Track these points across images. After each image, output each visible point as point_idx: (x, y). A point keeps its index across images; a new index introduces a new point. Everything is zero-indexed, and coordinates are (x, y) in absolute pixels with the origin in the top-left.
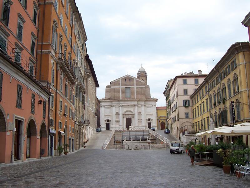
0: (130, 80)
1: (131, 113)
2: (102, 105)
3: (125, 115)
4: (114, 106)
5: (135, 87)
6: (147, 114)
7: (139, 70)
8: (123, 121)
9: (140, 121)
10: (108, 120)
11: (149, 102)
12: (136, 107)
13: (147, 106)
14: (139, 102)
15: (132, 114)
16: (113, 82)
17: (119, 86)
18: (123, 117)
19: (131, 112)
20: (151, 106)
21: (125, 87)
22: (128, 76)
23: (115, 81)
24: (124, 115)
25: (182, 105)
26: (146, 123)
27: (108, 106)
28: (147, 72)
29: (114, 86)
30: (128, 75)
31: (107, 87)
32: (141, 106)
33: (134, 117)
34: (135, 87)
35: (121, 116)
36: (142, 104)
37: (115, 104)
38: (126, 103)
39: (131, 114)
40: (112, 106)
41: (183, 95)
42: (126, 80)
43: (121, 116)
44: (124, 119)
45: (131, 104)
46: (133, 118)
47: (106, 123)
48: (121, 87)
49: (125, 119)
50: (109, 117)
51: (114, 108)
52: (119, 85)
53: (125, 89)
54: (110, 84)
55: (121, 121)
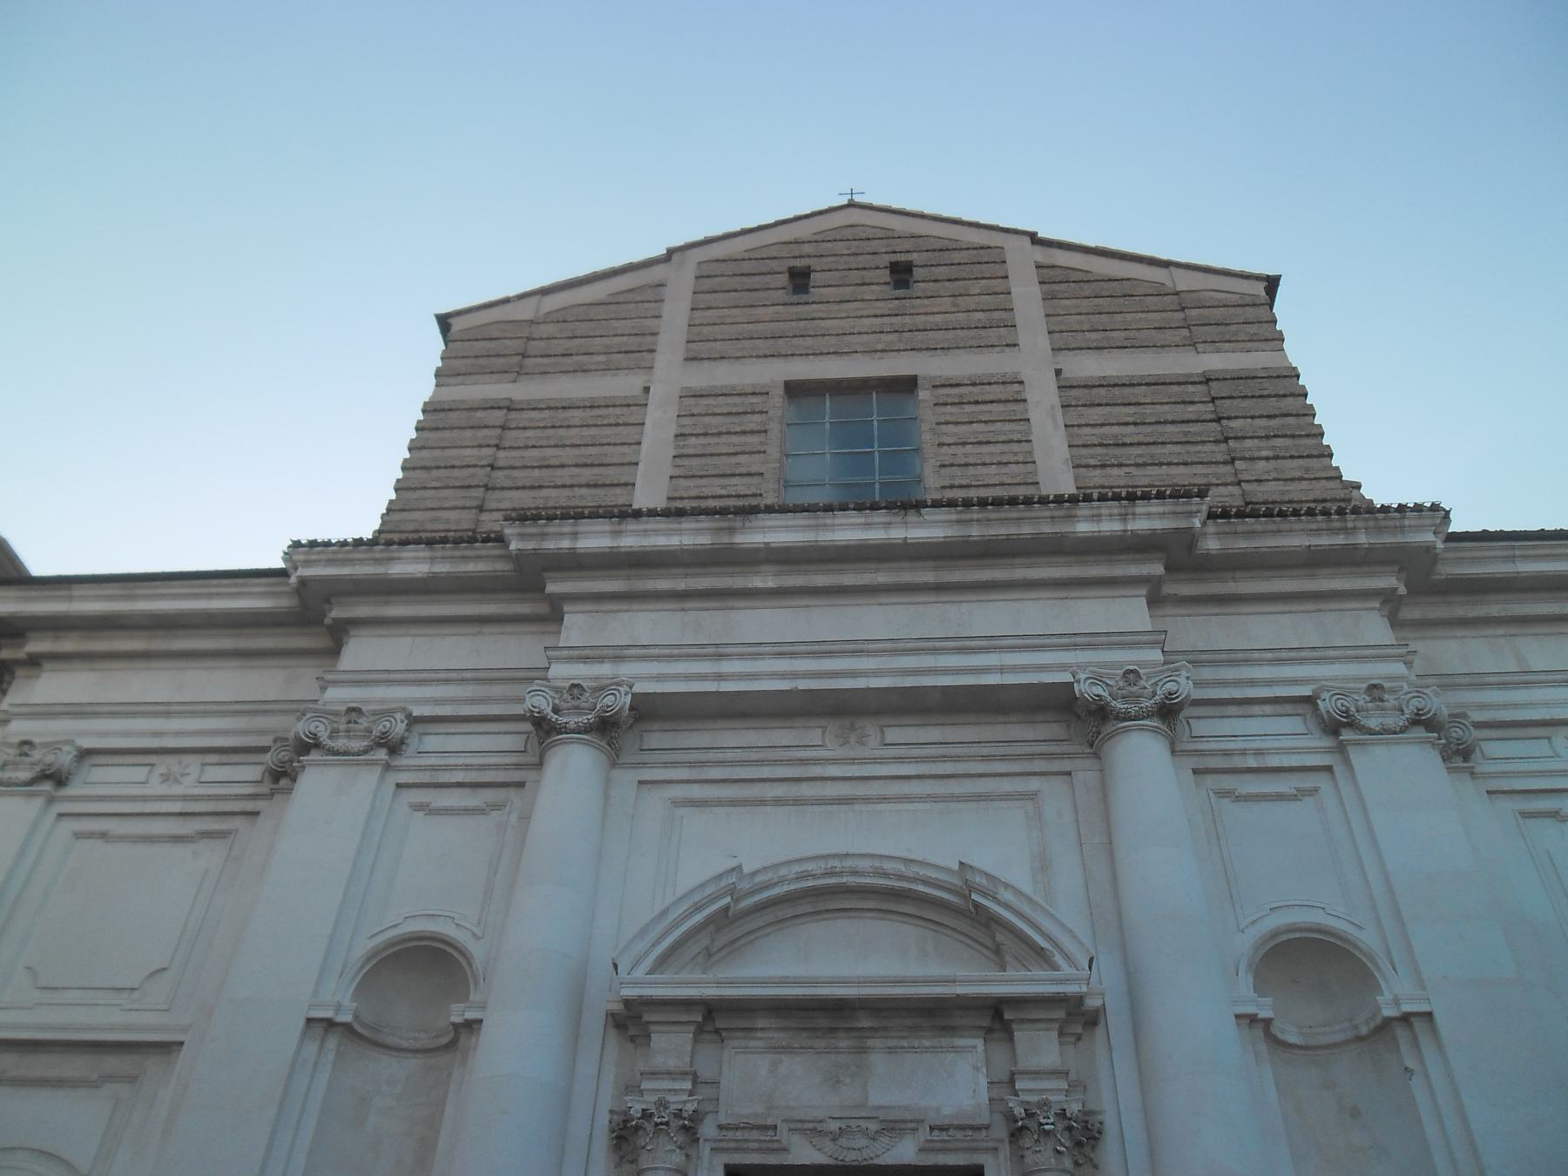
3: (716, 1018)
15: (997, 1017)
22: (855, 217)
24: (671, 1046)
27: (193, 778)
29: (519, 373)
30: (852, 205)
34: (1033, 361)
38: (768, 643)
39: (933, 1016)
42: (800, 279)
48: (670, 375)
52: (640, 353)
53: (778, 393)
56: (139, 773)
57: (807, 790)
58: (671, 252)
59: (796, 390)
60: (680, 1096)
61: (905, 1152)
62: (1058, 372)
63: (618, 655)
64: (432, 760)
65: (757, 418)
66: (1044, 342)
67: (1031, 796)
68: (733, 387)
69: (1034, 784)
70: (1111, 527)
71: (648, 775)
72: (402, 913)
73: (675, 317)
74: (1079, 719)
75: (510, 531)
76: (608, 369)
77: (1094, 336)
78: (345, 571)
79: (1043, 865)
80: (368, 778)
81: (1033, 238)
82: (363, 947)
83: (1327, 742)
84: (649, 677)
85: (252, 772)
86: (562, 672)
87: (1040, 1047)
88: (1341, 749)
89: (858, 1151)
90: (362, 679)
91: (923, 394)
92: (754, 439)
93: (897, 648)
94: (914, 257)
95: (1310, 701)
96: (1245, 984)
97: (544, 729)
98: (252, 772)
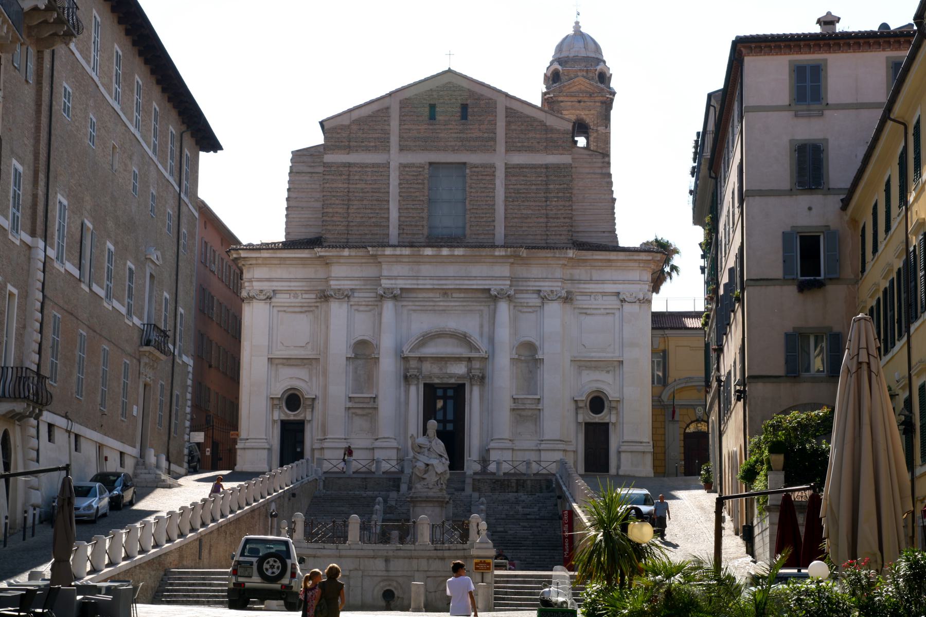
0: (464, 107)
1: (463, 352)
2: (266, 286)
3: (421, 359)
4: (346, 296)
5: (500, 159)
6: (583, 364)
7: (560, 48)
8: (402, 406)
9: (527, 412)
10: (293, 400)
11: (596, 275)
12: (503, 307)
13: (581, 301)
14: (522, 271)
15: (469, 359)
16: (338, 122)
17: (387, 149)
18: (407, 379)
19: (463, 339)
20: (613, 302)
21: (421, 158)
23: (355, 115)
25: (778, 273)
26: (572, 426)
28: (612, 60)
29: (349, 149)
30: (450, 71)
31: (300, 157)
32: (534, 300)
33: (482, 379)
34: (500, 159)
35: (388, 366)
36: (546, 286)
37: (347, 285)
39: (459, 359)
40: (324, 297)
41: (790, 192)
42: (432, 107)
43: (388, 366)
44: (413, 389)
45: (467, 284)
46: (476, 390)
47: (278, 415)
48: (396, 158)
49: (416, 395)
50: (302, 373)
51: (338, 311)
52: (383, 144)
53: (427, 167)
54: (317, 138)
55: (386, 408)
56: (288, 296)
57: (436, 308)
58: (390, 95)
59: (431, 164)
60: (415, 372)
61: (453, 381)
62: (506, 164)
63: (396, 278)
64: (356, 299)
65: (421, 177)
66: (503, 149)
67: (482, 311)
68: (414, 164)
69: (482, 308)
70: (503, 253)
71: (405, 303)
72: (359, 335)
73: (394, 125)
74: (490, 297)
75: (370, 249)
76: (376, 149)
77: (519, 144)
78: (331, 254)
79: (481, 326)
80: (345, 306)
81: (507, 95)
82: (353, 342)
83: (539, 301)
84: (402, 284)
85: (313, 296)
86: (385, 283)
87: (476, 365)
88: (543, 303)
89: (445, 381)
90: (337, 279)
91: (468, 171)
92: (421, 186)
93: (455, 278)
94: (469, 102)
95: (540, 291)
96: (514, 352)
97: (382, 297)
98: (313, 296)
